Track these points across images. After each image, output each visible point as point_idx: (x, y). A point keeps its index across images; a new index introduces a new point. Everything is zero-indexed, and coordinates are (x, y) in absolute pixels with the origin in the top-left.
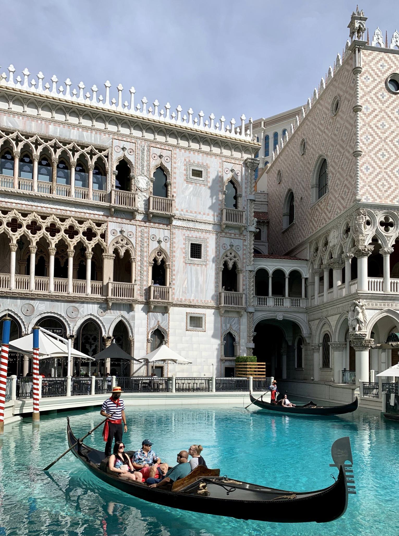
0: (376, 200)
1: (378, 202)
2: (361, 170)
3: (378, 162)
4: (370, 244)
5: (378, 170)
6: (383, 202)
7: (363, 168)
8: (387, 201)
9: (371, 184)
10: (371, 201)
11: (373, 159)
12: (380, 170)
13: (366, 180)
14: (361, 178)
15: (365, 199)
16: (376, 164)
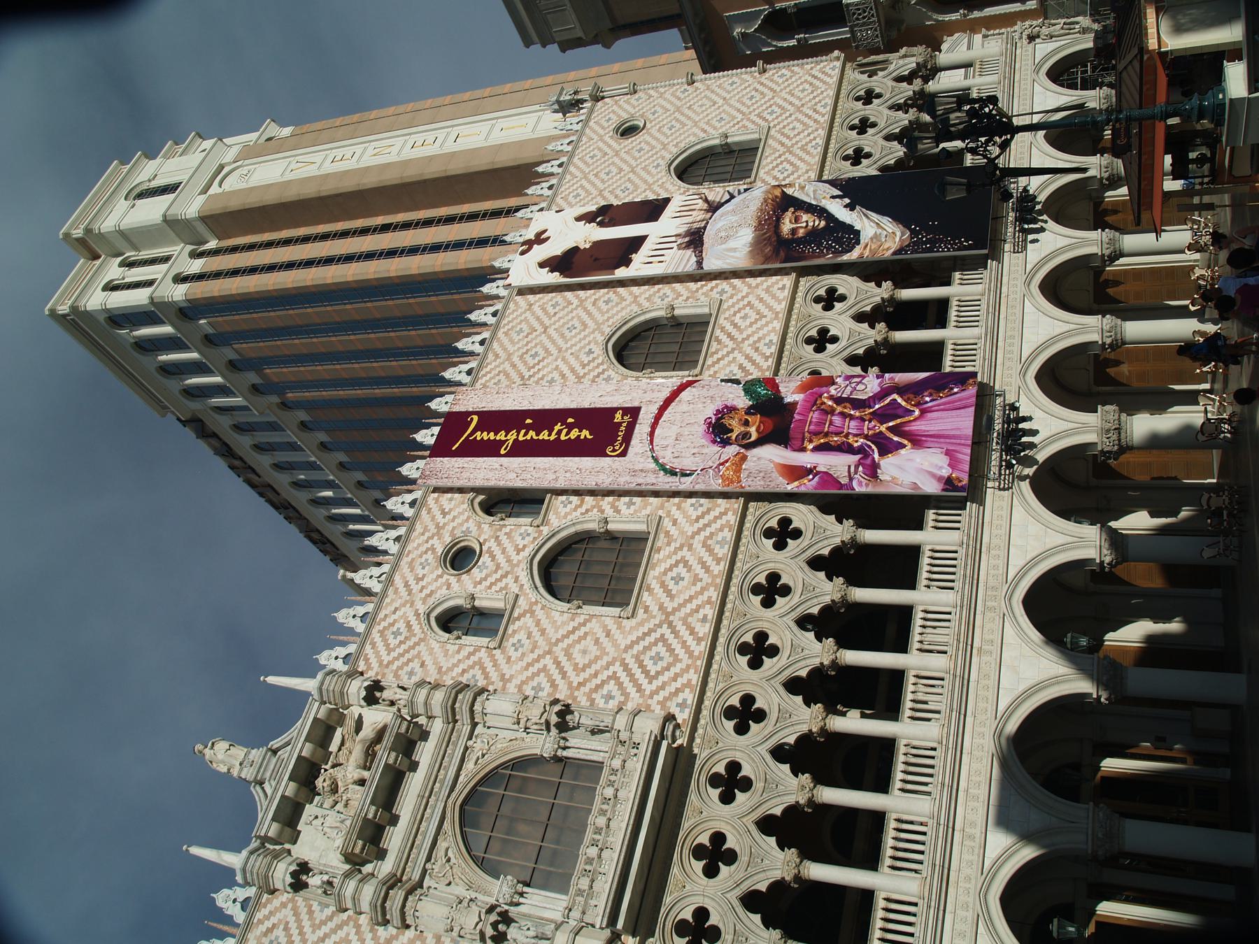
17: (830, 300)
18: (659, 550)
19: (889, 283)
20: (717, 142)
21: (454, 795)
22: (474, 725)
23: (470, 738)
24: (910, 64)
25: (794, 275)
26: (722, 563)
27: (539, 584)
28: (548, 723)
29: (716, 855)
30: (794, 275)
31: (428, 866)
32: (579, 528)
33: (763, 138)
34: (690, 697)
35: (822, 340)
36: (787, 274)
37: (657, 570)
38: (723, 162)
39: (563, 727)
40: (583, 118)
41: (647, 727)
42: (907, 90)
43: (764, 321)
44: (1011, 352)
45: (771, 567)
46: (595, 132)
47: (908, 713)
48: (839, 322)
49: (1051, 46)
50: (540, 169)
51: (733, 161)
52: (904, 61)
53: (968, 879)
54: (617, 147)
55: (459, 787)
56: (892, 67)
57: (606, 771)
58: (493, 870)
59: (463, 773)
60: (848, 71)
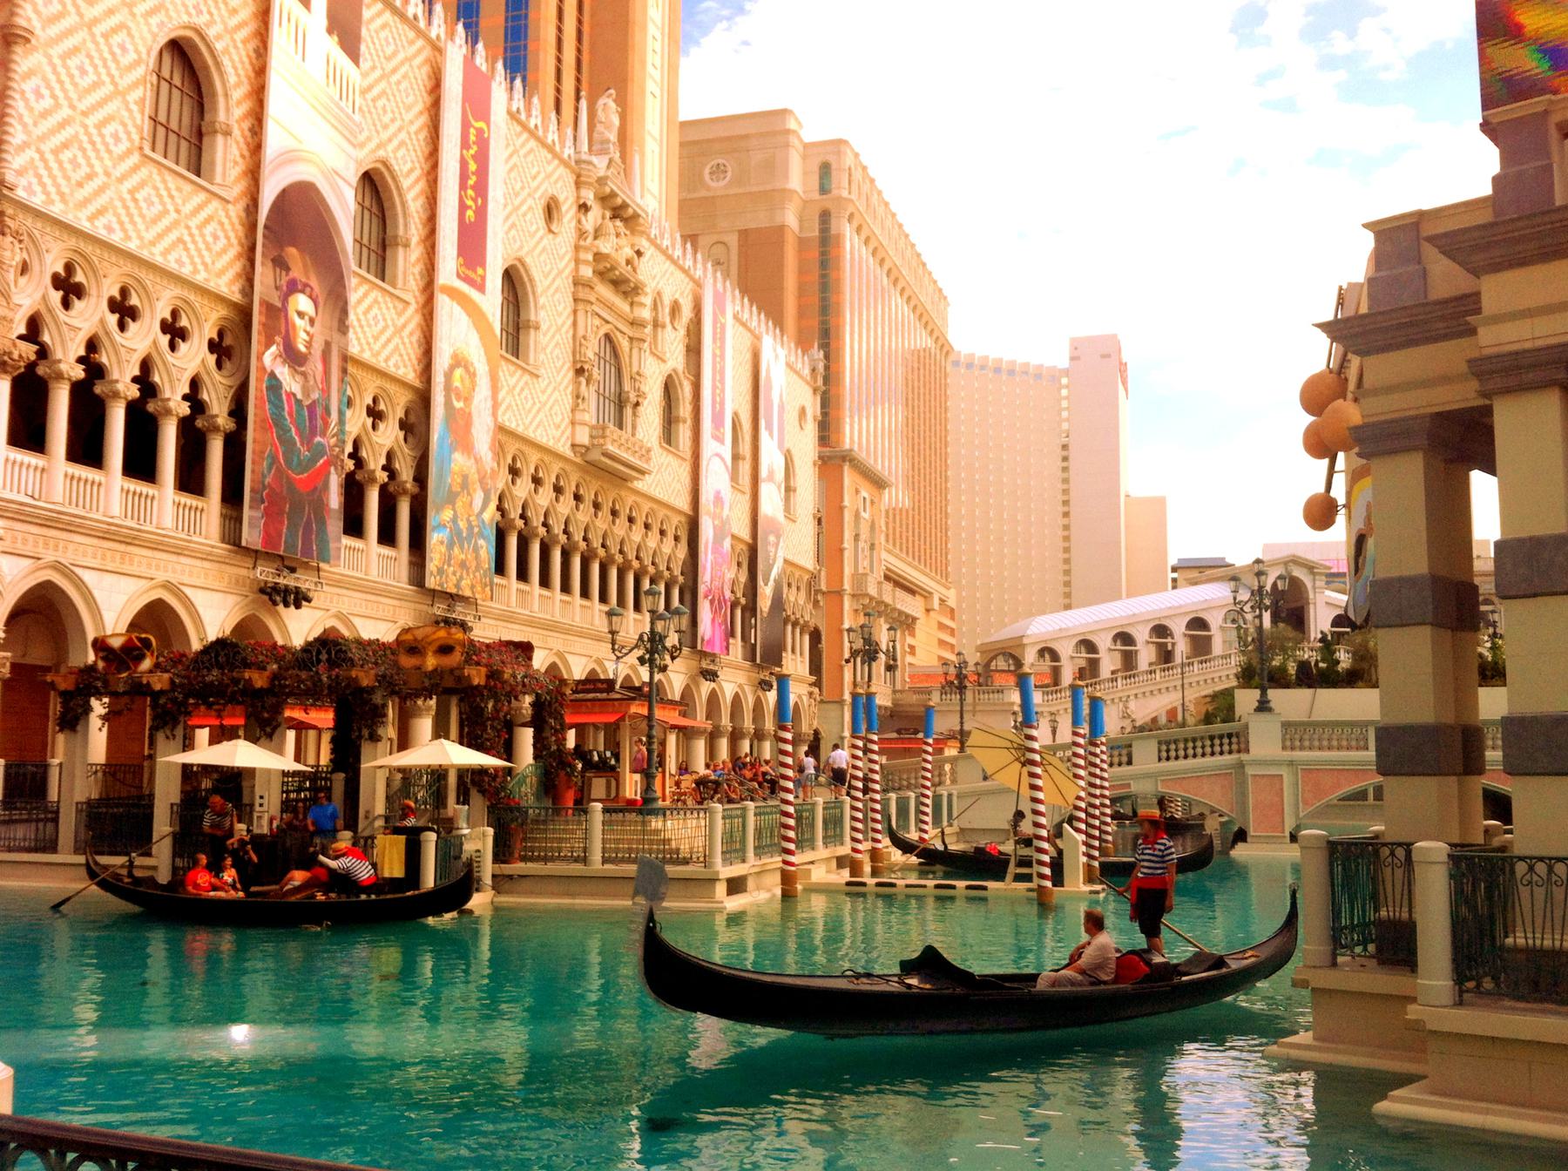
0: (52, 202)
1: (56, 210)
2: (23, 92)
3: (69, 86)
4: (21, 337)
5: (65, 112)
6: (70, 216)
7: (28, 86)
8: (80, 215)
9: (43, 147)
10: (37, 201)
11: (51, 63)
12: (70, 112)
13: (31, 127)
14: (21, 117)
15: (25, 189)
16: (64, 90)
17: (174, 332)
18: (160, 174)
19: (188, 411)
26: (87, 225)
27: (197, 40)
33: (396, 292)
35: (68, 288)
38: (374, 234)
43: (141, 227)
44: (25, 541)
45: (92, 289)
46: (523, 145)
48: (143, 337)
50: (518, 82)
51: (373, 247)
54: (537, 196)
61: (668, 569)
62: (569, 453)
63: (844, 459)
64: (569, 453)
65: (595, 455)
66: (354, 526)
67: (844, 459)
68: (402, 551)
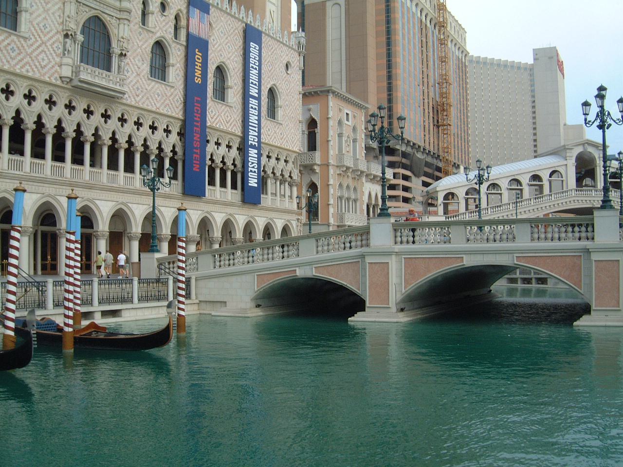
20: (279, 104)
21: (101, 13)
22: (119, 19)
23: (116, 18)
24: (295, 177)
25: (241, 135)
28: (123, 50)
29: (89, 112)
30: (241, 135)
31: (81, 4)
32: (171, 55)
34: (128, 102)
36: (242, 133)
37: (156, 86)
39: (121, 55)
40: (294, 47)
41: (125, 89)
42: (287, 175)
47: (53, 164)
49: (295, 226)
52: (296, 176)
53: (91, 195)
55: (103, 14)
56: (295, 170)
57: (108, 73)
58: (83, 32)
59: (106, 16)
60: (295, 155)
61: (290, 176)
62: (59, 83)
63: (328, 91)
64: (59, 83)
65: (76, 83)
66: (212, 182)
67: (328, 91)
68: (239, 191)
